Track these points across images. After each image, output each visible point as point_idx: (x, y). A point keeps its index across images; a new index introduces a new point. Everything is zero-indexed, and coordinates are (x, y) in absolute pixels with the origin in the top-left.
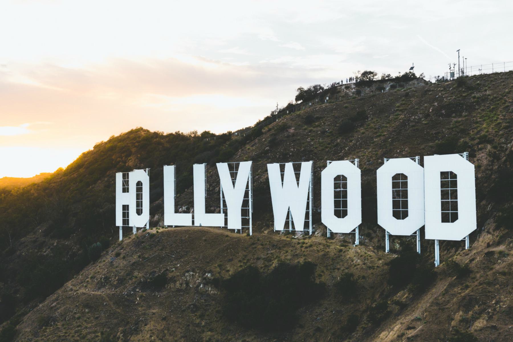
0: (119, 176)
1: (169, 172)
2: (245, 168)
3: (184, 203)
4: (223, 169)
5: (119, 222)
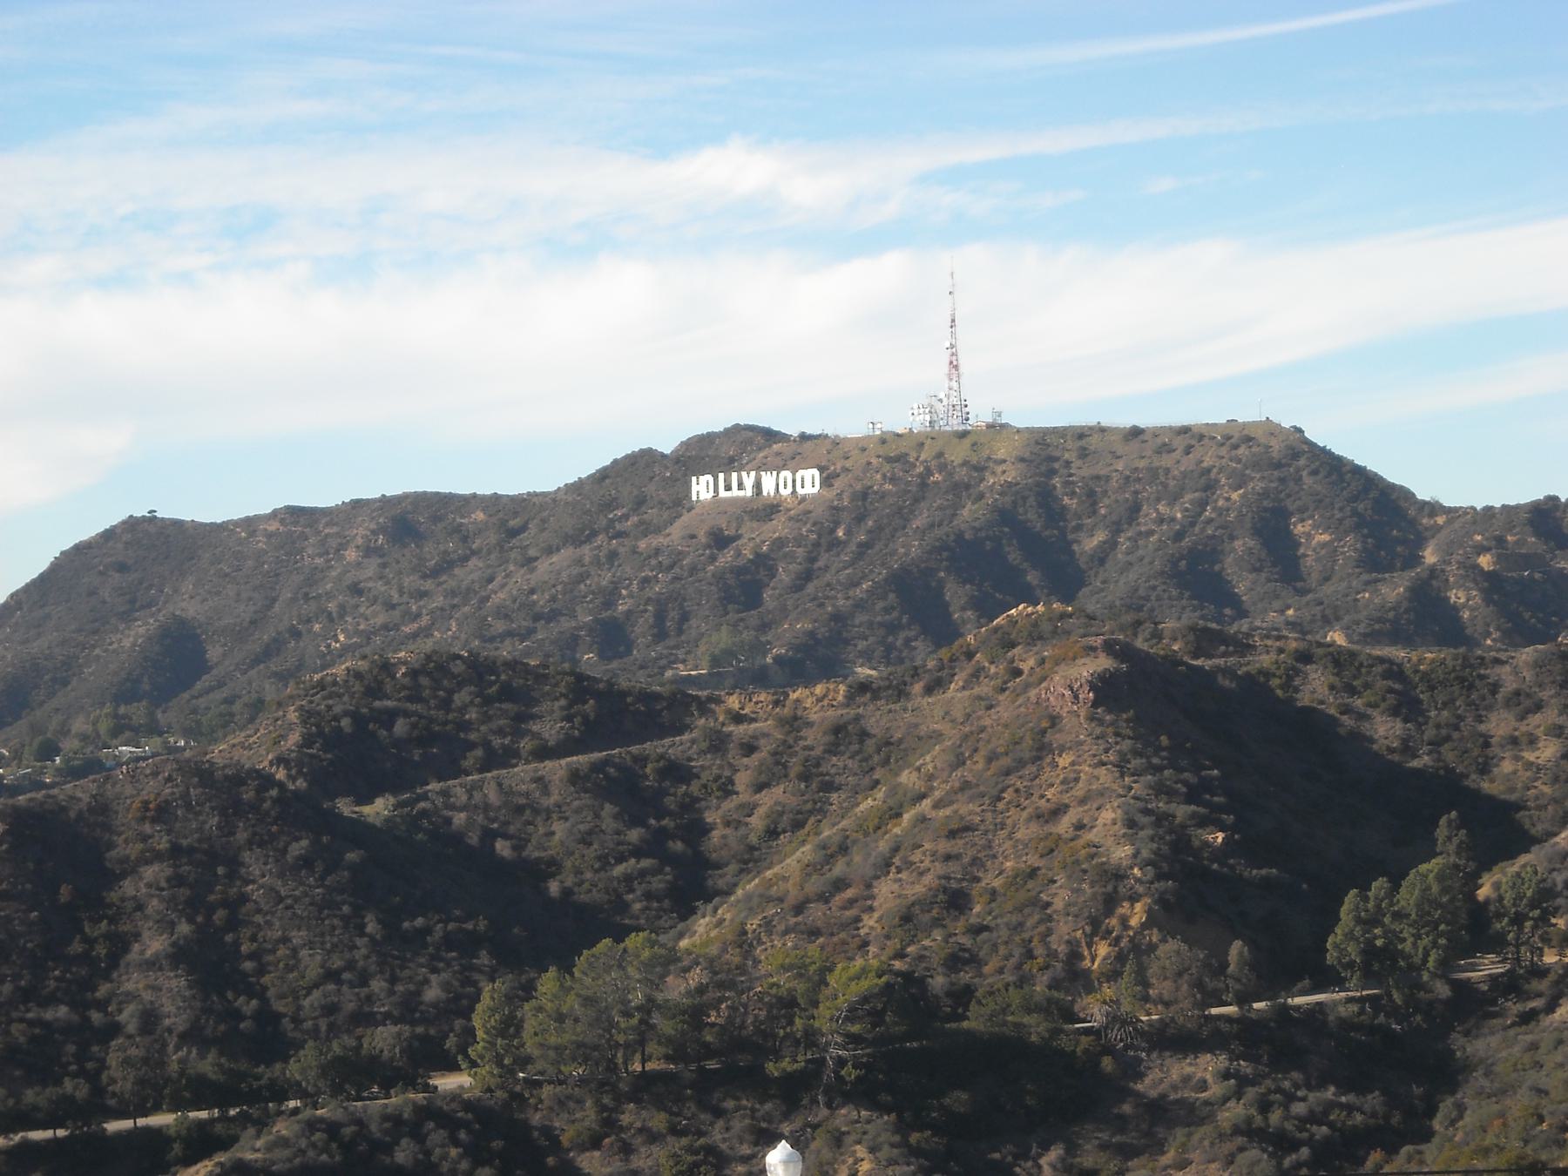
0: (694, 479)
1: (721, 476)
2: (753, 474)
3: (728, 488)
4: (744, 474)
5: (694, 498)
